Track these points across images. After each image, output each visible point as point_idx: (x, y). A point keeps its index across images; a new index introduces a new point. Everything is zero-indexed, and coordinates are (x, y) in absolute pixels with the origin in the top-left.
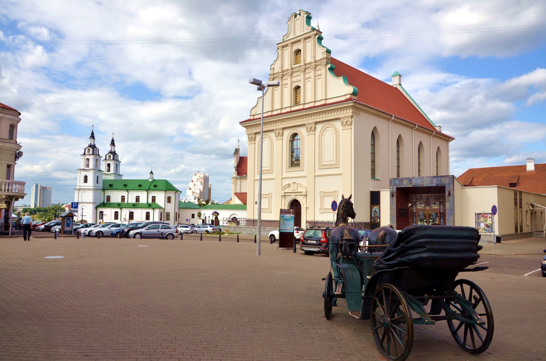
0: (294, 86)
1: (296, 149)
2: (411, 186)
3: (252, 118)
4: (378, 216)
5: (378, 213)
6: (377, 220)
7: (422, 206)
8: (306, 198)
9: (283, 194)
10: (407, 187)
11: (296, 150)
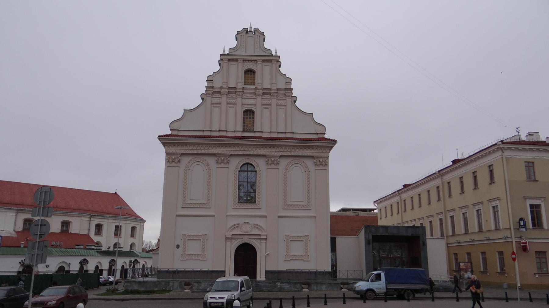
0: (245, 109)
1: (246, 182)
2: (387, 234)
3: (175, 133)
8: (266, 243)
9: (230, 237)
10: (383, 235)
11: (245, 184)
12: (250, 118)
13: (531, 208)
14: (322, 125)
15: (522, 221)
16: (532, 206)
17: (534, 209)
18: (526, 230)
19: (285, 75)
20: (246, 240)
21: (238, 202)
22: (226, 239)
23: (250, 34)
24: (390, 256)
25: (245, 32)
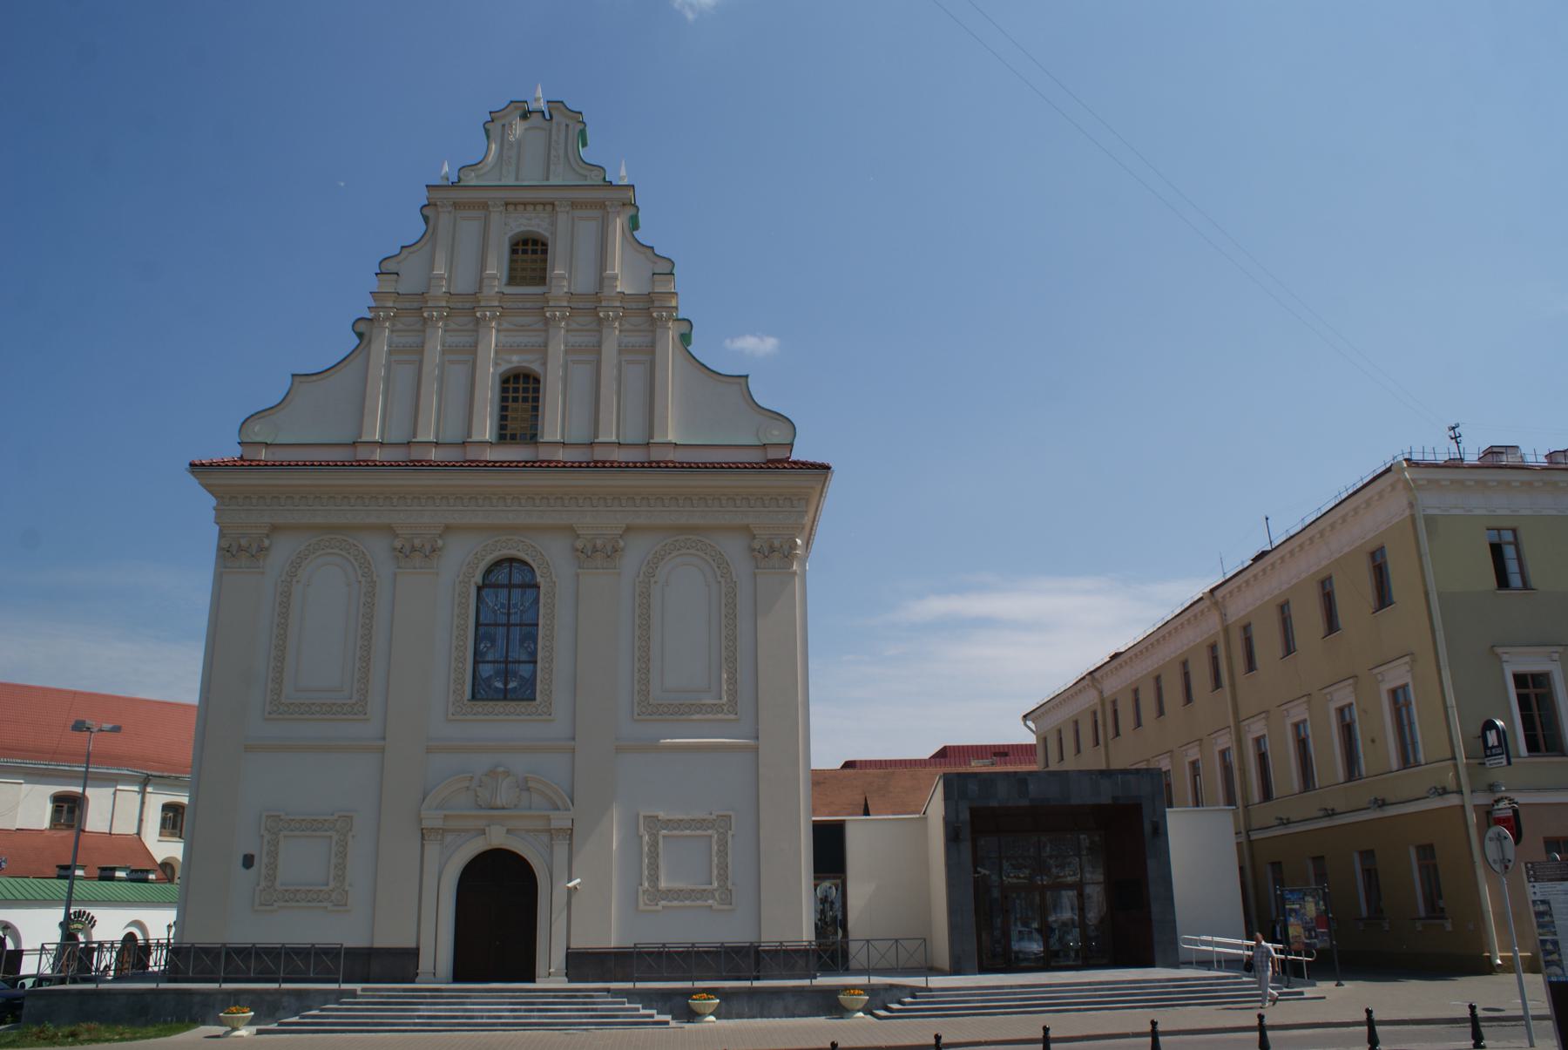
0: (504, 367)
2: (1024, 803)
4: (840, 917)
5: (838, 905)
6: (836, 933)
7: (1022, 876)
11: (501, 631)
12: (525, 400)
13: (1517, 686)
14: (782, 416)
15: (1494, 732)
16: (1520, 679)
17: (1528, 687)
18: (1509, 763)
19: (652, 248)
20: (498, 838)
21: (474, 697)
22: (423, 834)
23: (535, 119)
24: (1039, 883)
25: (519, 112)
